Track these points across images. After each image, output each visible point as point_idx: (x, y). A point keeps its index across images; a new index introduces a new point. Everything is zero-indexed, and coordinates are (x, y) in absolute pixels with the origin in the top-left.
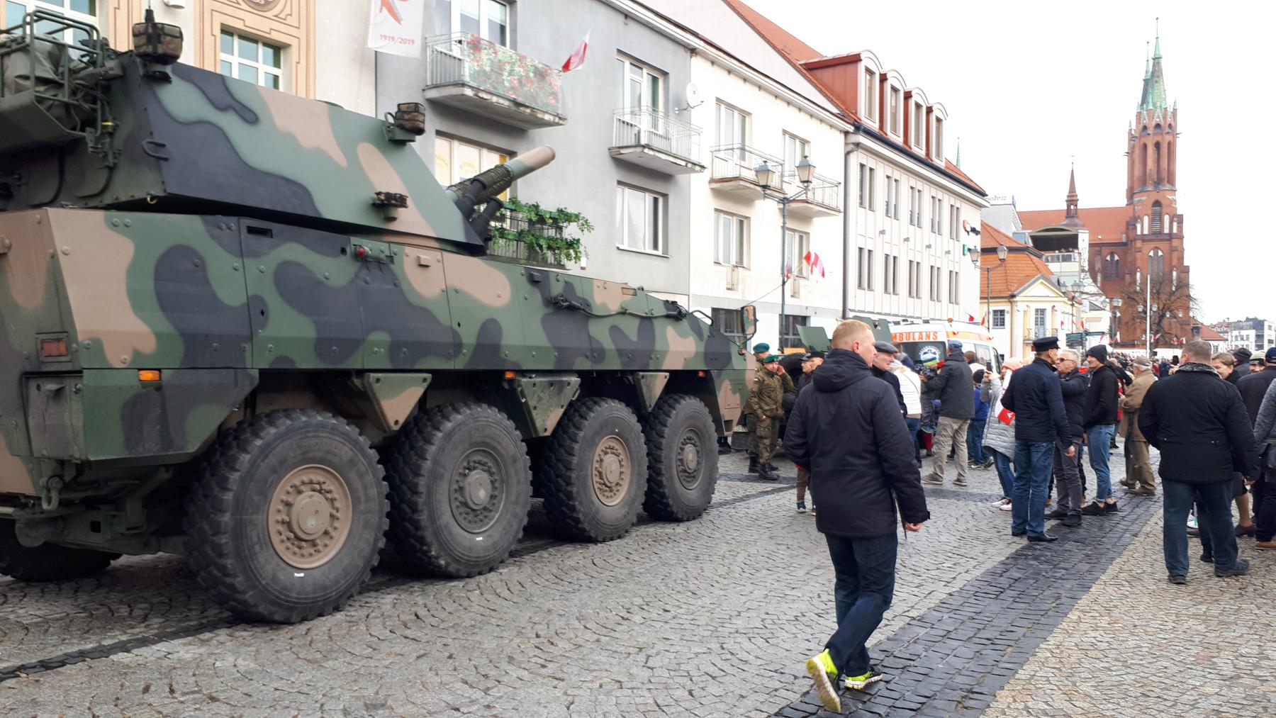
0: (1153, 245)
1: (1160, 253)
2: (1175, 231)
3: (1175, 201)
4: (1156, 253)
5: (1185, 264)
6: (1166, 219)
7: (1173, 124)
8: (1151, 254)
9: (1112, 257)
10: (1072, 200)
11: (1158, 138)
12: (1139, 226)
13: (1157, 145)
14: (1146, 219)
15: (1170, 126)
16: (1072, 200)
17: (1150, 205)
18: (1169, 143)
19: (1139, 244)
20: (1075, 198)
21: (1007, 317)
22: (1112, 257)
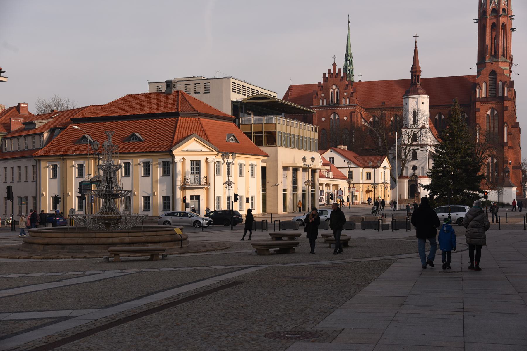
1: (495, 112)
2: (506, 95)
7: (506, 8)
8: (489, 113)
10: (415, 70)
12: (478, 91)
14: (484, 85)
15: (504, 10)
16: (415, 70)
17: (488, 75)
21: (171, 166)
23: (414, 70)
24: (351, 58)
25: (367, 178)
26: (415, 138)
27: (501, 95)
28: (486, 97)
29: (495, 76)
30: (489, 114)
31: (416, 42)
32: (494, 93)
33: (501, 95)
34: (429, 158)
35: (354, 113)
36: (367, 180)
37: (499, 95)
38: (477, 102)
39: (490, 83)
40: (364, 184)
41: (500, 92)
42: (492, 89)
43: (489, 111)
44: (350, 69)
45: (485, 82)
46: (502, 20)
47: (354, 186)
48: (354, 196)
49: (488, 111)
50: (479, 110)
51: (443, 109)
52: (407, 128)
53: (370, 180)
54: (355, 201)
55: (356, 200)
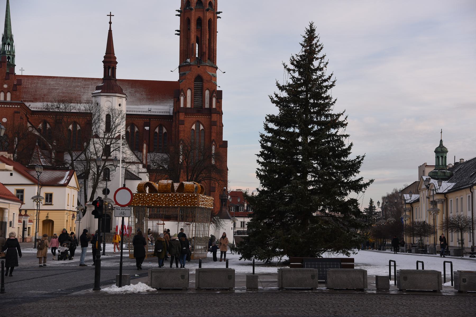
0: (195, 118)
1: (202, 127)
2: (214, 106)
3: (215, 77)
4: (197, 127)
5: (224, 139)
6: (207, 92)
7: (213, 2)
8: (194, 127)
9: (161, 130)
11: (200, 14)
12: (182, 99)
13: (199, 22)
14: (189, 93)
17: (193, 80)
18: (210, 21)
19: (182, 117)
20: (112, 60)
22: (161, 130)
23: (107, 60)
24: (12, 41)
25: (47, 201)
26: (107, 150)
27: (208, 107)
28: (191, 108)
29: (201, 83)
30: (194, 129)
31: (110, 23)
32: (199, 103)
33: (208, 107)
34: (125, 179)
35: (19, 114)
36: (45, 205)
37: (206, 107)
38: (181, 113)
39: (195, 91)
40: (41, 211)
41: (207, 103)
42: (198, 99)
43: (194, 124)
44: (10, 56)
45: (189, 88)
46: (209, 15)
47: (26, 213)
48: (26, 228)
49: (193, 125)
50: (182, 123)
51: (137, 119)
52: (97, 136)
53: (51, 205)
54: (26, 236)
55: (28, 235)
